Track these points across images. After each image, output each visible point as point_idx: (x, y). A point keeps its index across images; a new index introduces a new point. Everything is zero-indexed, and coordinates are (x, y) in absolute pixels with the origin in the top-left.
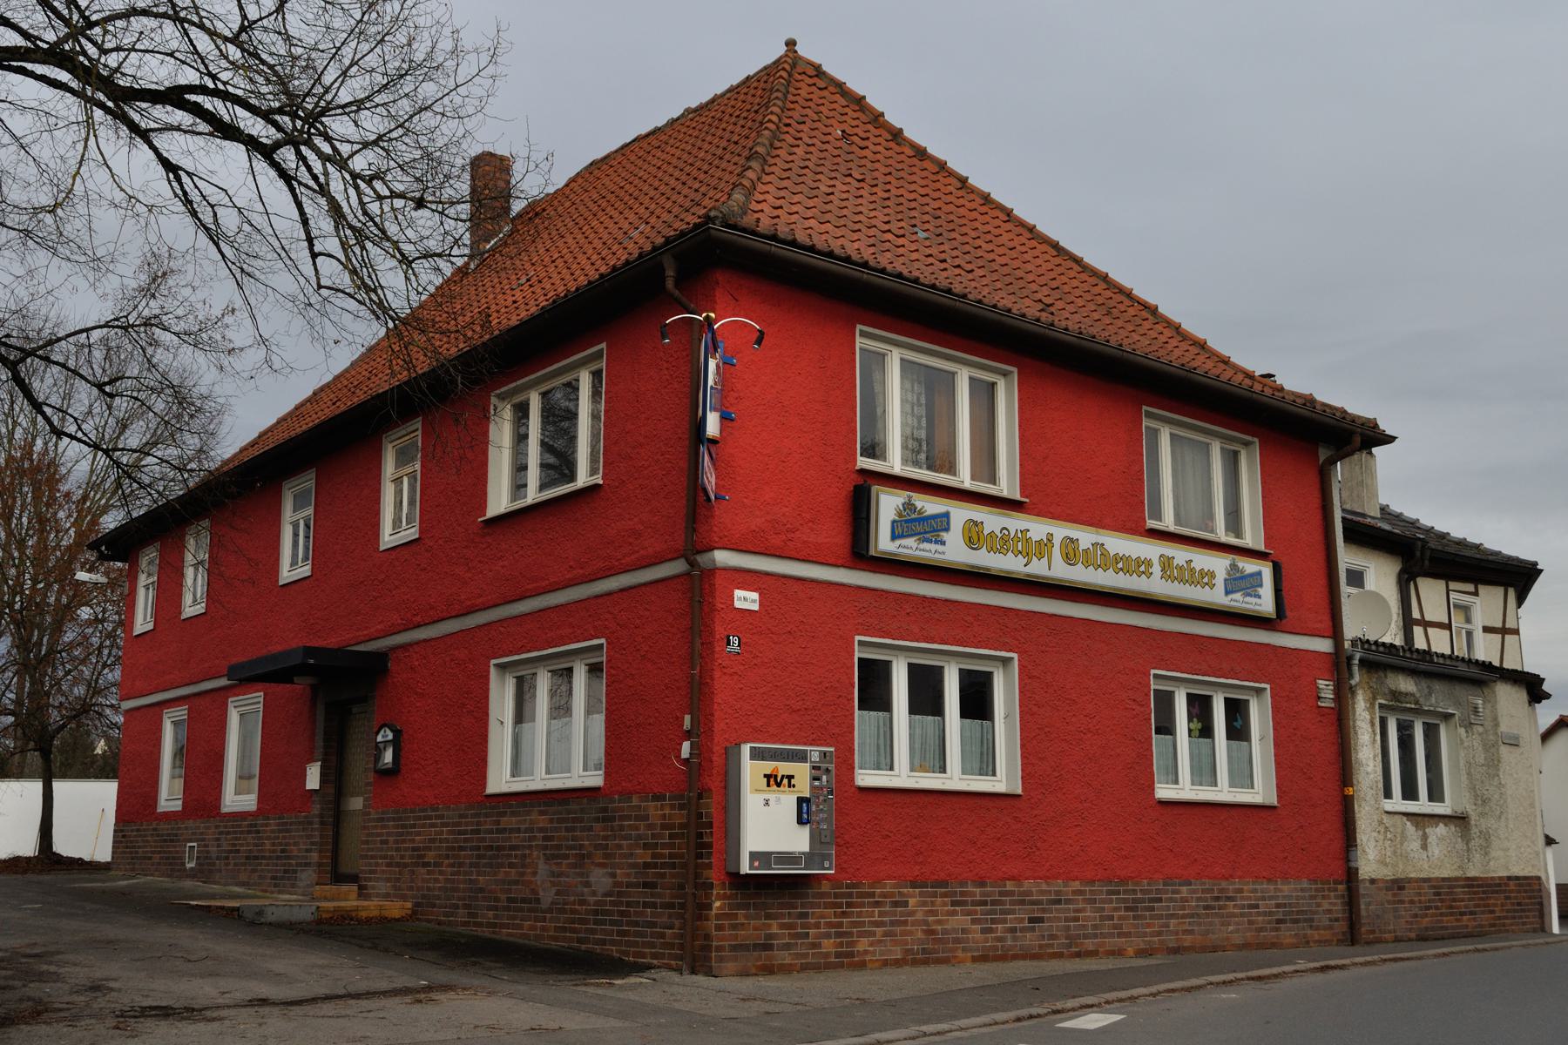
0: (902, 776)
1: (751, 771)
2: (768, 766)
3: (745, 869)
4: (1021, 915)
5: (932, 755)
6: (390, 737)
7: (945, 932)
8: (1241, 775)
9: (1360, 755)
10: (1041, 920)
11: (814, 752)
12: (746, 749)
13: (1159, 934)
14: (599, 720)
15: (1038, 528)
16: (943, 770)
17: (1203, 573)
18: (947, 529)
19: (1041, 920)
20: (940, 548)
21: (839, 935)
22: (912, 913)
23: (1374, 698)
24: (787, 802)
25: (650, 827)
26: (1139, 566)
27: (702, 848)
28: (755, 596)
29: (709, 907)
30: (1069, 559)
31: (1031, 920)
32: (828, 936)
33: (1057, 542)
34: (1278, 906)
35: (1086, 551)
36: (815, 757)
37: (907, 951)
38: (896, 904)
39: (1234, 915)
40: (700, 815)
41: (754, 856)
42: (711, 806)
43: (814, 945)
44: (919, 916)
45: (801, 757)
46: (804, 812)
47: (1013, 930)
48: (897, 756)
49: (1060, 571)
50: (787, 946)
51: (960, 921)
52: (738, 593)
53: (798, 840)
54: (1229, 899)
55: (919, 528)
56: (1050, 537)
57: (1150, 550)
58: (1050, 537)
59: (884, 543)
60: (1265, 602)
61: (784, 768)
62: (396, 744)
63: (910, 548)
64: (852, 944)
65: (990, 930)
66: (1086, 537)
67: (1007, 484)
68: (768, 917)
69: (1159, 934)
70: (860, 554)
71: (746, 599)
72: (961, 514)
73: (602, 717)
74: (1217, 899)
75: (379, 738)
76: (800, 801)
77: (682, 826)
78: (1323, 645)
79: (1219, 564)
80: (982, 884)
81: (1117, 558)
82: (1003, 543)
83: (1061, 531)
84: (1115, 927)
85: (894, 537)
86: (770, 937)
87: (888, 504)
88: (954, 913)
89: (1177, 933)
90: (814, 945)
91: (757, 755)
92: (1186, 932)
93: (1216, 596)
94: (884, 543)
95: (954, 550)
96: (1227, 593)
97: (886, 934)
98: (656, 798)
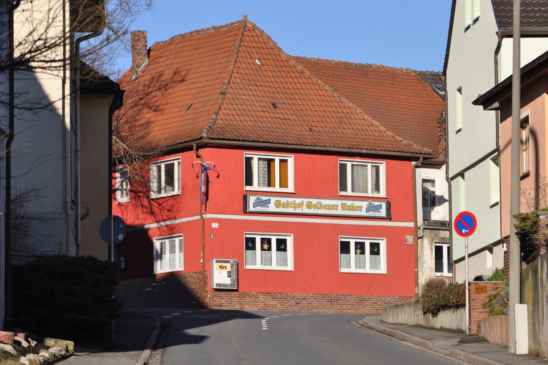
0: (353, 269)
1: (216, 266)
2: (220, 264)
3: (215, 287)
4: (293, 302)
5: (359, 264)
6: (123, 259)
7: (270, 305)
8: (374, 265)
9: (425, 259)
10: (299, 303)
11: (232, 261)
12: (214, 260)
13: (339, 309)
14: (182, 255)
15: (298, 201)
16: (350, 267)
17: (357, 207)
18: (270, 203)
19: (299, 303)
20: (267, 208)
21: (240, 304)
22: (260, 300)
23: (433, 240)
24: (225, 272)
25: (195, 279)
26: (335, 207)
27: (205, 283)
28: (217, 224)
29: (207, 296)
30: (308, 207)
31: (296, 303)
32: (237, 304)
33: (305, 203)
34: (385, 303)
35: (315, 205)
36: (232, 262)
37: (259, 309)
38: (256, 297)
39: (367, 305)
40: (205, 276)
41: (217, 284)
42: (207, 274)
43: (233, 306)
44: (262, 301)
45: (228, 262)
46: (229, 275)
47: (291, 305)
48: (256, 261)
49: (306, 210)
50: (227, 306)
51: (274, 302)
52: (213, 224)
53: (228, 281)
54: (365, 300)
55: (261, 204)
56: (302, 202)
57: (338, 202)
58: (302, 202)
59: (251, 208)
60: (383, 213)
61: (224, 265)
62: (126, 261)
63: (259, 209)
64: (244, 306)
65: (283, 305)
66: (314, 201)
67: (291, 188)
68: (222, 299)
69: (339, 309)
70: (245, 212)
71: (215, 225)
72: (273, 199)
73: (183, 253)
74: (361, 300)
75: (120, 260)
76: (228, 272)
77: (202, 279)
78: (411, 224)
79: (364, 204)
80: (281, 293)
81: (325, 206)
82: (287, 205)
83: (306, 200)
84: (324, 306)
85: (254, 207)
86: (222, 303)
87: (252, 199)
88: (273, 300)
89: (346, 309)
90: (233, 306)
91: (217, 262)
92: (349, 309)
93: (363, 213)
94: (251, 208)
95: (272, 208)
96: (367, 212)
97: (253, 304)
98: (196, 272)
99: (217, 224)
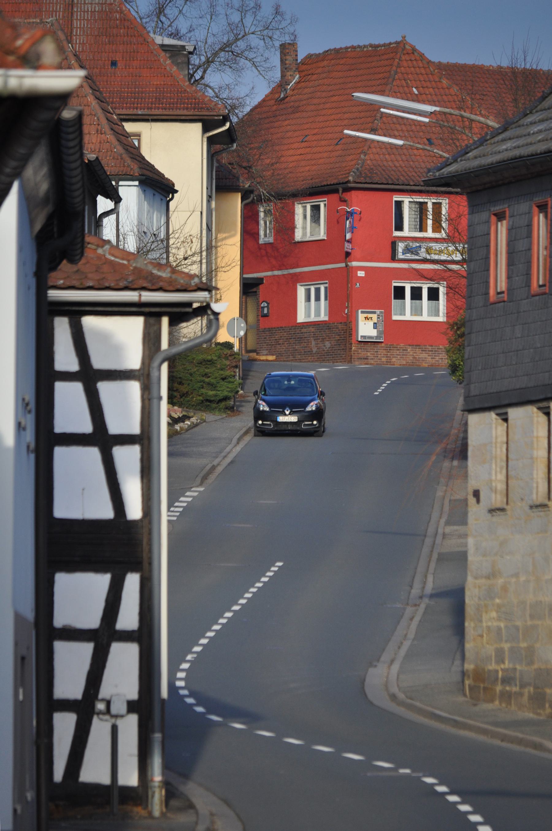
1: (361, 317)
2: (365, 315)
3: (360, 340)
7: (419, 358)
11: (378, 311)
12: (360, 311)
21: (387, 357)
22: (409, 353)
24: (371, 324)
25: (339, 330)
28: (364, 272)
29: (351, 349)
32: (384, 357)
37: (407, 362)
38: (404, 350)
41: (361, 336)
43: (380, 359)
44: (411, 354)
45: (375, 313)
46: (375, 326)
47: (442, 359)
48: (406, 312)
50: (372, 359)
51: (424, 355)
52: (359, 272)
53: (374, 333)
59: (400, 256)
61: (370, 315)
62: (267, 307)
63: (409, 256)
68: (367, 351)
70: (393, 258)
71: (361, 274)
76: (374, 323)
77: (346, 330)
80: (432, 346)
85: (403, 254)
87: (401, 246)
88: (422, 353)
90: (380, 359)
91: (362, 312)
98: (341, 323)
99: (364, 272)
